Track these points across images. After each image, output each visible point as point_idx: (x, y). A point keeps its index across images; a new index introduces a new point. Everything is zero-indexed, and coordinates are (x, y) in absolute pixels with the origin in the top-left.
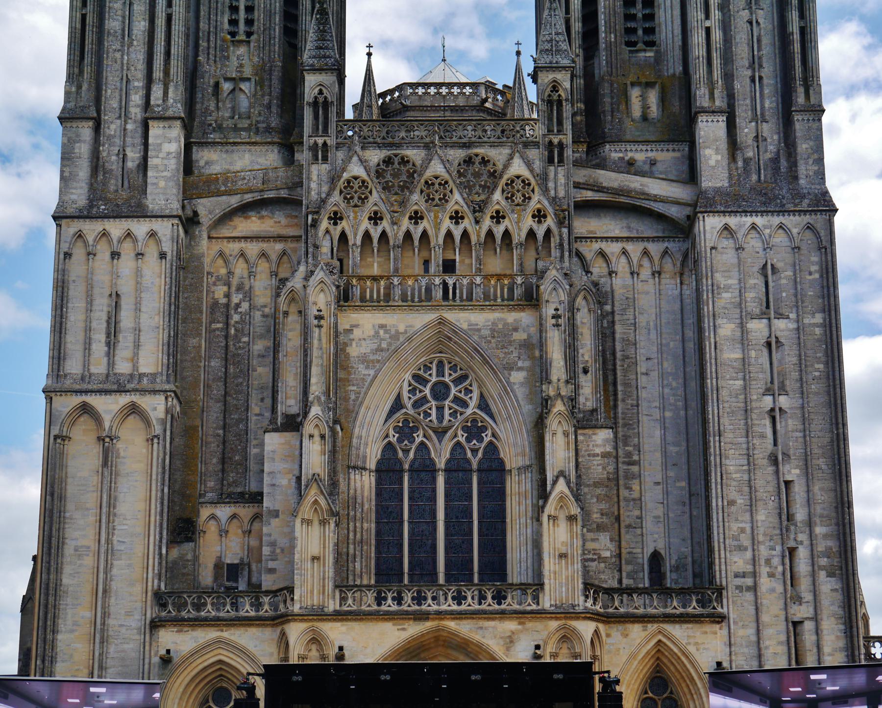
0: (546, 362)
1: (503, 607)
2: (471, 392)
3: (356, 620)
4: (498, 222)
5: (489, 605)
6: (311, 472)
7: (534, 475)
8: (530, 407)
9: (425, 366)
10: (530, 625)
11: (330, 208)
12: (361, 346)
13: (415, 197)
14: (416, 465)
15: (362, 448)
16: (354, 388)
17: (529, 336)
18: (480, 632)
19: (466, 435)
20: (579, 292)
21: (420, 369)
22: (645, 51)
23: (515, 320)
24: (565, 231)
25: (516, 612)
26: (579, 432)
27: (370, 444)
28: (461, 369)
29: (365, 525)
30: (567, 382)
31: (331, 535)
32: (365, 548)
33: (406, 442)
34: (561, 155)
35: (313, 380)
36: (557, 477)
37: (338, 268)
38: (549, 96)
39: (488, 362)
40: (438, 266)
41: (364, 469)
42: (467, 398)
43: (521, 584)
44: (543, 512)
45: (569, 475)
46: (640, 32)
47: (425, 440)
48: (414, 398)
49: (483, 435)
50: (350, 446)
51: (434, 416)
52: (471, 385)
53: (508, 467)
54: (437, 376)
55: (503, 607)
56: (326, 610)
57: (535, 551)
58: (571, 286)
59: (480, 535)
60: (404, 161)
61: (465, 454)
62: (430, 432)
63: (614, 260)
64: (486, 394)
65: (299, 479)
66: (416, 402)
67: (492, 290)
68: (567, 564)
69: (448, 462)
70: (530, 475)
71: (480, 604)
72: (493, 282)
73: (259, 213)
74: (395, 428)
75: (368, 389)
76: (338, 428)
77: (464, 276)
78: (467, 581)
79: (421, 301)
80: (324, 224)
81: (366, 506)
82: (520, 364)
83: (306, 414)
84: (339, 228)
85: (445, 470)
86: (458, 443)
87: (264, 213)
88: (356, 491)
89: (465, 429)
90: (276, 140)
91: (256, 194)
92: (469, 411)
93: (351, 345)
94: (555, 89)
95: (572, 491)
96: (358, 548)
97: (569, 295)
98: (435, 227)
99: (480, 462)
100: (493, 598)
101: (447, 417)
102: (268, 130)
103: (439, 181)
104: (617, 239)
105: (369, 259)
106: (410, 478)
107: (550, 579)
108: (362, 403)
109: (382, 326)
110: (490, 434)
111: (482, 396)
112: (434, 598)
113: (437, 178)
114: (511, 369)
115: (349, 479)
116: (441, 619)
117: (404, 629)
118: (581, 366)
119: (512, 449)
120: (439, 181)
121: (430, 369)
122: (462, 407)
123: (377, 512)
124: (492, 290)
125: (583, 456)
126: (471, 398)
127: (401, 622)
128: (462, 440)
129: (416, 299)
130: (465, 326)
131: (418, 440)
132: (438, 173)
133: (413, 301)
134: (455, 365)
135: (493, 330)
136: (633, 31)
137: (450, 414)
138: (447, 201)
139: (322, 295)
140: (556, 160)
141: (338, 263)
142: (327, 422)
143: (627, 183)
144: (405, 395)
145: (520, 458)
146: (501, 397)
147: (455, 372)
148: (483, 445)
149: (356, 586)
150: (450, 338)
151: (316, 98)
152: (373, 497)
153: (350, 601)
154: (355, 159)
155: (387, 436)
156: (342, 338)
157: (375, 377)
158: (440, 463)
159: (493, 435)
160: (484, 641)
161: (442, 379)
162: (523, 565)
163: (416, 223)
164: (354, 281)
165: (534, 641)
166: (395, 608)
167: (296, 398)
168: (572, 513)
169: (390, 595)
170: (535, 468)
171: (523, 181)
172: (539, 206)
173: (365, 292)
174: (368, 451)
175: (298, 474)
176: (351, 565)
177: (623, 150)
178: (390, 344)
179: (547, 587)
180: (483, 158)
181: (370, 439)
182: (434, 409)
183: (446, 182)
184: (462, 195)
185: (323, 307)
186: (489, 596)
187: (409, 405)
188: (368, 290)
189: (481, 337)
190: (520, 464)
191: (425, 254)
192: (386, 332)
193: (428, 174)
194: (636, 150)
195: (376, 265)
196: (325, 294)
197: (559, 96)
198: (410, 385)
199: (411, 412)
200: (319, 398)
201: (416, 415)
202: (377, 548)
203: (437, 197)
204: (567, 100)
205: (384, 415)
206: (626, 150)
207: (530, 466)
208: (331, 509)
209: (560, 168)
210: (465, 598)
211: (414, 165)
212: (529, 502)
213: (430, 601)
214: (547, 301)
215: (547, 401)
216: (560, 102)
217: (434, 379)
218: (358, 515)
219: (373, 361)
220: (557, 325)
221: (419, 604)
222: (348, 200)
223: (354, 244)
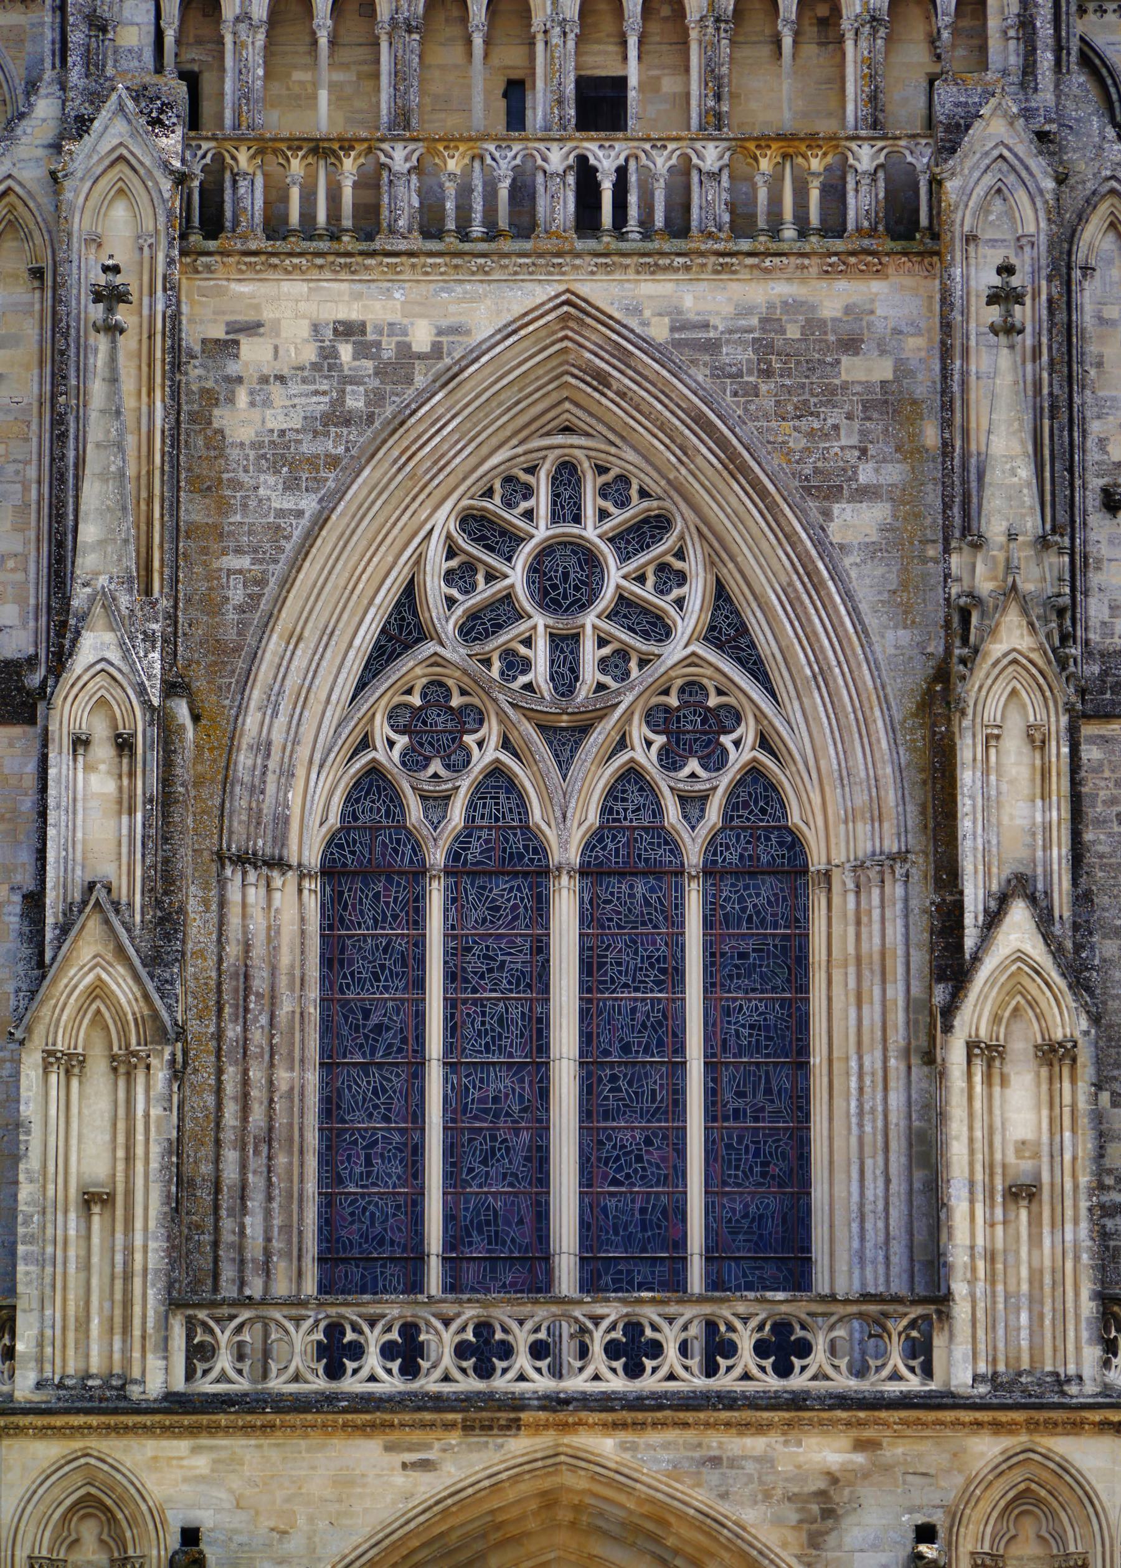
0: (965, 467)
1: (798, 1382)
2: (682, 578)
3: (247, 1430)
5: (746, 1376)
6: (79, 876)
7: (915, 889)
8: (904, 636)
9: (509, 480)
10: (896, 1451)
12: (267, 403)
14: (474, 853)
15: (271, 788)
16: (244, 562)
17: (902, 370)
18: (712, 1476)
19: (660, 740)
20: (1091, 203)
21: (489, 493)
23: (848, 310)
25: (843, 1401)
26: (1088, 730)
27: (301, 772)
28: (643, 494)
29: (283, 1077)
30: (1043, 543)
31: (156, 1112)
32: (281, 1160)
33: (436, 766)
35: (89, 532)
36: (1004, 900)
37: (183, 108)
39: (744, 469)
40: (560, 102)
41: (279, 864)
42: (664, 603)
43: (866, 1298)
44: (948, 1029)
45: (1048, 894)
47: (506, 758)
48: (467, 603)
49: (726, 740)
50: (227, 782)
51: (540, 672)
52: (680, 555)
53: (817, 861)
54: (556, 517)
55: (798, 1382)
56: (134, 1391)
57: (918, 1175)
58: (1061, 180)
59: (711, 1115)
61: (658, 811)
62: (528, 729)
64: (735, 587)
65: (34, 901)
66: (473, 616)
67: (762, 194)
68: (1035, 1222)
69: (596, 840)
70: (899, 891)
71: (711, 1370)
72: (765, 164)
74: (392, 716)
75: (296, 564)
76: (182, 710)
77: (658, 144)
78: (664, 1286)
79: (492, 234)
81: (286, 1007)
82: (866, 475)
83: (60, 660)
85: (584, 872)
86: (632, 775)
88: (247, 947)
89: (658, 718)
92: (674, 652)
93: (231, 400)
95: (1056, 951)
96: (254, 1163)
97: (1055, 212)
99: (713, 845)
100: (761, 1349)
101: (590, 673)
105: (298, 76)
106: (452, 901)
107: (972, 1282)
108: (269, 620)
109: (347, 330)
110: (750, 739)
111: (721, 594)
112: (538, 1350)
114: (834, 493)
115: (222, 904)
116: (564, 1427)
117: (425, 1465)
118: (1096, 483)
119: (834, 795)
121: (528, 492)
122: (646, 635)
123: (327, 1028)
124: (762, 194)
125: (1100, 822)
126: (680, 603)
127: (417, 1436)
128: (647, 759)
129: (477, 230)
130: (659, 331)
131: (482, 760)
133: (463, 234)
134: (623, 479)
135: (763, 347)
137: (604, 665)
139: (120, 212)
141: (182, 88)
142: (142, 691)
144: (434, 588)
145: (863, 829)
146: (794, 601)
147: (623, 503)
148: (725, 780)
149: (249, 1302)
150: (603, 379)
152: (314, 972)
153: (224, 1361)
155: (365, 743)
156: (195, 373)
157: (321, 521)
158: (564, 845)
159: (764, 743)
160: (724, 1508)
161: (574, 530)
162: (874, 1228)
164: (243, 157)
165: (911, 1510)
166: (392, 1384)
167: (21, 601)
168: (1059, 1035)
169: (374, 1339)
170: (920, 867)
173: (285, 199)
174: (294, 797)
175: (30, 885)
176: (228, 1224)
178: (377, 399)
179: (961, 1310)
181: (303, 752)
182: (542, 644)
185: (122, 256)
186: (745, 1340)
187: (449, 628)
188: (295, 193)
189: (719, 373)
190: (864, 847)
192: (363, 350)
195: (323, 95)
196: (133, 205)
198: (451, 554)
199: (455, 652)
200: (109, 601)
201: (476, 667)
202: (326, 1159)
205: (355, 665)
207: (901, 856)
208: (155, 1016)
210: (656, 1349)
212: (896, 992)
213: (523, 1361)
214: (971, 239)
215: (965, 615)
217: (542, 531)
218: (257, 1037)
219: (312, 461)
220: (1009, 329)
221: (485, 1371)
223: (244, 17)
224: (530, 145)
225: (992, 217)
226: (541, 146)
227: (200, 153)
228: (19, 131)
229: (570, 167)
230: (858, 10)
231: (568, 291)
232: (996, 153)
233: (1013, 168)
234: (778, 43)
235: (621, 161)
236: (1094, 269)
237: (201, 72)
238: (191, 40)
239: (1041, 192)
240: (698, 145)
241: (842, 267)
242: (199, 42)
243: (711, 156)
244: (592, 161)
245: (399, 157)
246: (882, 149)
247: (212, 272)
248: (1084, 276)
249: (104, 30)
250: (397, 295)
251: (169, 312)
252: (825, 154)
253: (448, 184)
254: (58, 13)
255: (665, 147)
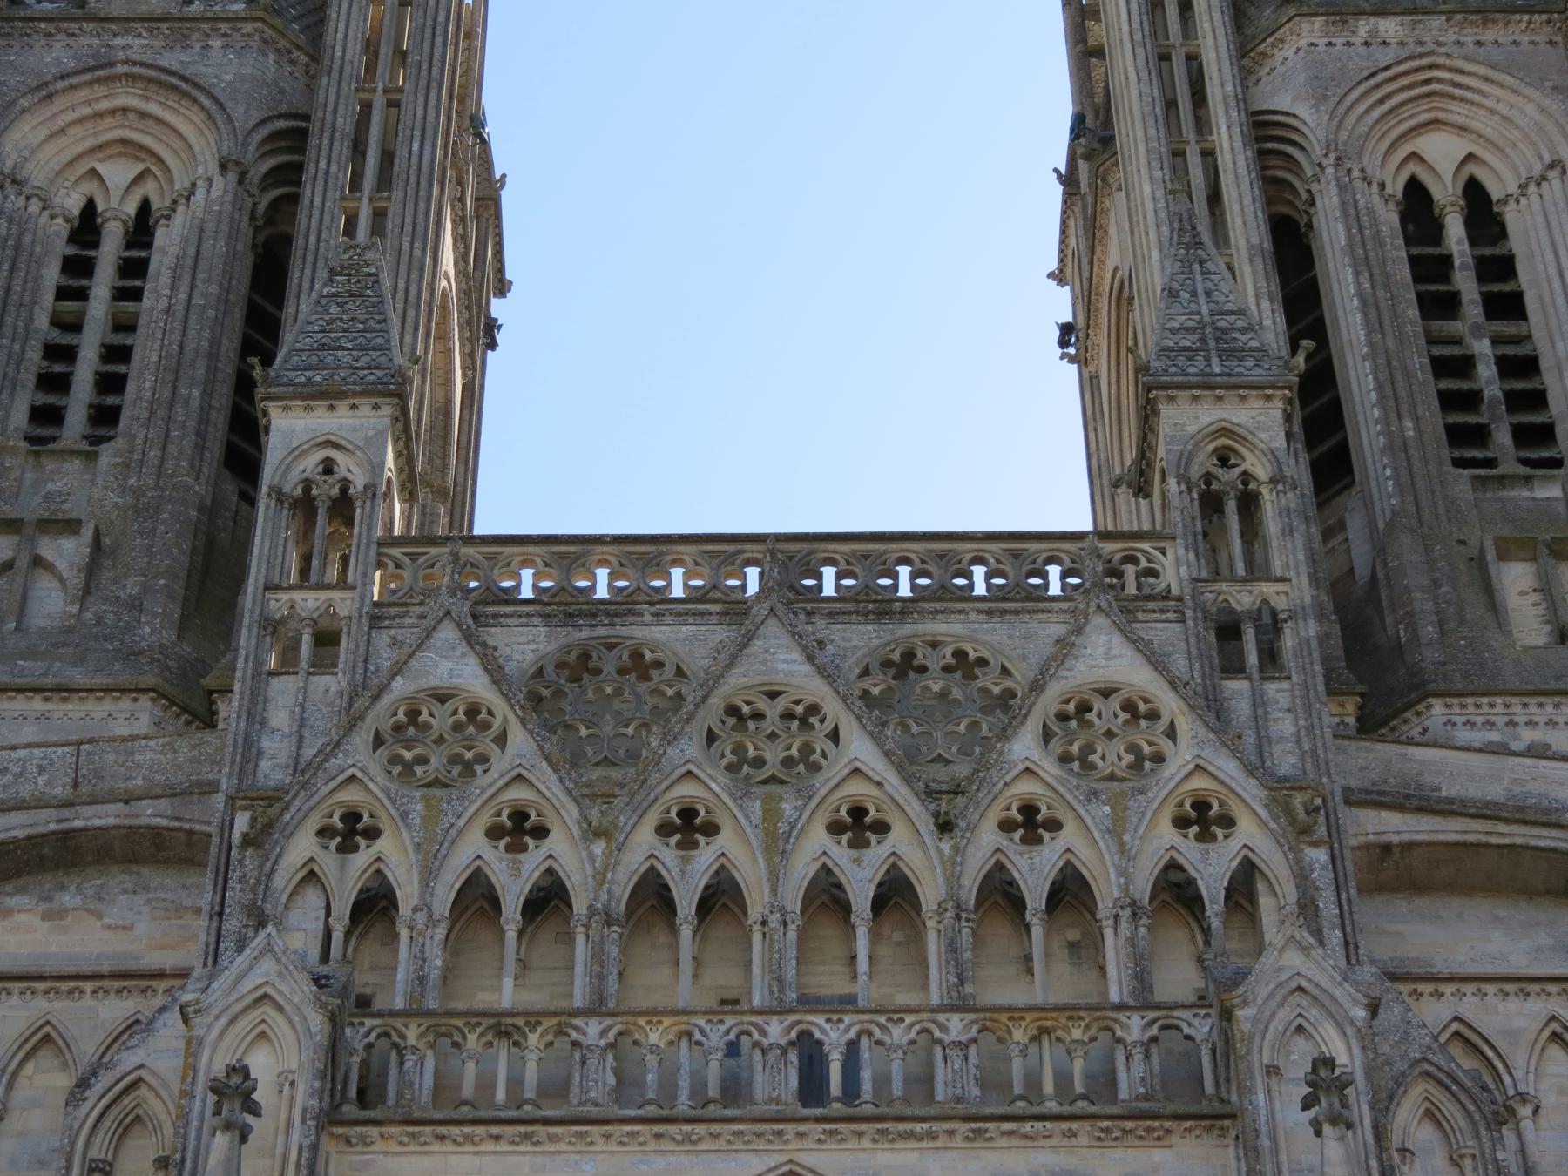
4: (1032, 839)
11: (333, 801)
13: (689, 749)
20: (1400, 1081)
22: (1528, 479)
24: (1319, 856)
34: (1270, 657)
38: (1208, 478)
46: (1502, 437)
60: (640, 665)
63: (1518, 1059)
73: (48, 899)
77: (896, 1013)
80: (302, 847)
84: (361, 859)
87: (68, 899)
90: (149, 680)
91: (44, 814)
94: (1224, 460)
98: (768, 850)
102: (130, 655)
103: (782, 704)
104: (1523, 982)
113: (773, 695)
120: (782, 704)
129: (683, 1104)
132: (780, 677)
136: (1480, 435)
138: (816, 768)
140: (1252, 658)
143: (1537, 787)
151: (307, 484)
154: (448, 633)
163: (688, 845)
171: (1128, 706)
172: (1199, 783)
177: (1500, 721)
180: (960, 654)
183: (813, 709)
184: (880, 745)
191: (723, 977)
193: (738, 683)
194: (1551, 723)
197: (1246, 477)
203: (773, 755)
204: (1273, 481)
206: (1512, 723)
209: (1271, 687)
211: (680, 672)
214: (1272, 1071)
216: (1249, 503)
222: (408, 768)
223: (424, 907)
224: (747, 1018)
225: (1293, 1057)
226: (758, 1019)
227: (363, 1030)
228: (158, 1024)
229: (792, 1044)
230: (1116, 894)
231: (791, 1161)
232: (1294, 984)
233: (1314, 998)
234: (1028, 959)
235: (852, 1034)
236: (1413, 1154)
237: (373, 995)
238: (366, 966)
239: (1352, 1023)
240: (941, 1017)
241: (1118, 1134)
242: (374, 968)
243: (956, 1027)
244: (818, 1035)
245: (592, 1030)
246: (1153, 1022)
247: (367, 1145)
248: (1403, 1160)
249: (261, 924)
250: (586, 1167)
251: (307, 1142)
252: (1088, 1027)
253: (649, 1057)
254: (216, 918)
255: (902, 1020)
